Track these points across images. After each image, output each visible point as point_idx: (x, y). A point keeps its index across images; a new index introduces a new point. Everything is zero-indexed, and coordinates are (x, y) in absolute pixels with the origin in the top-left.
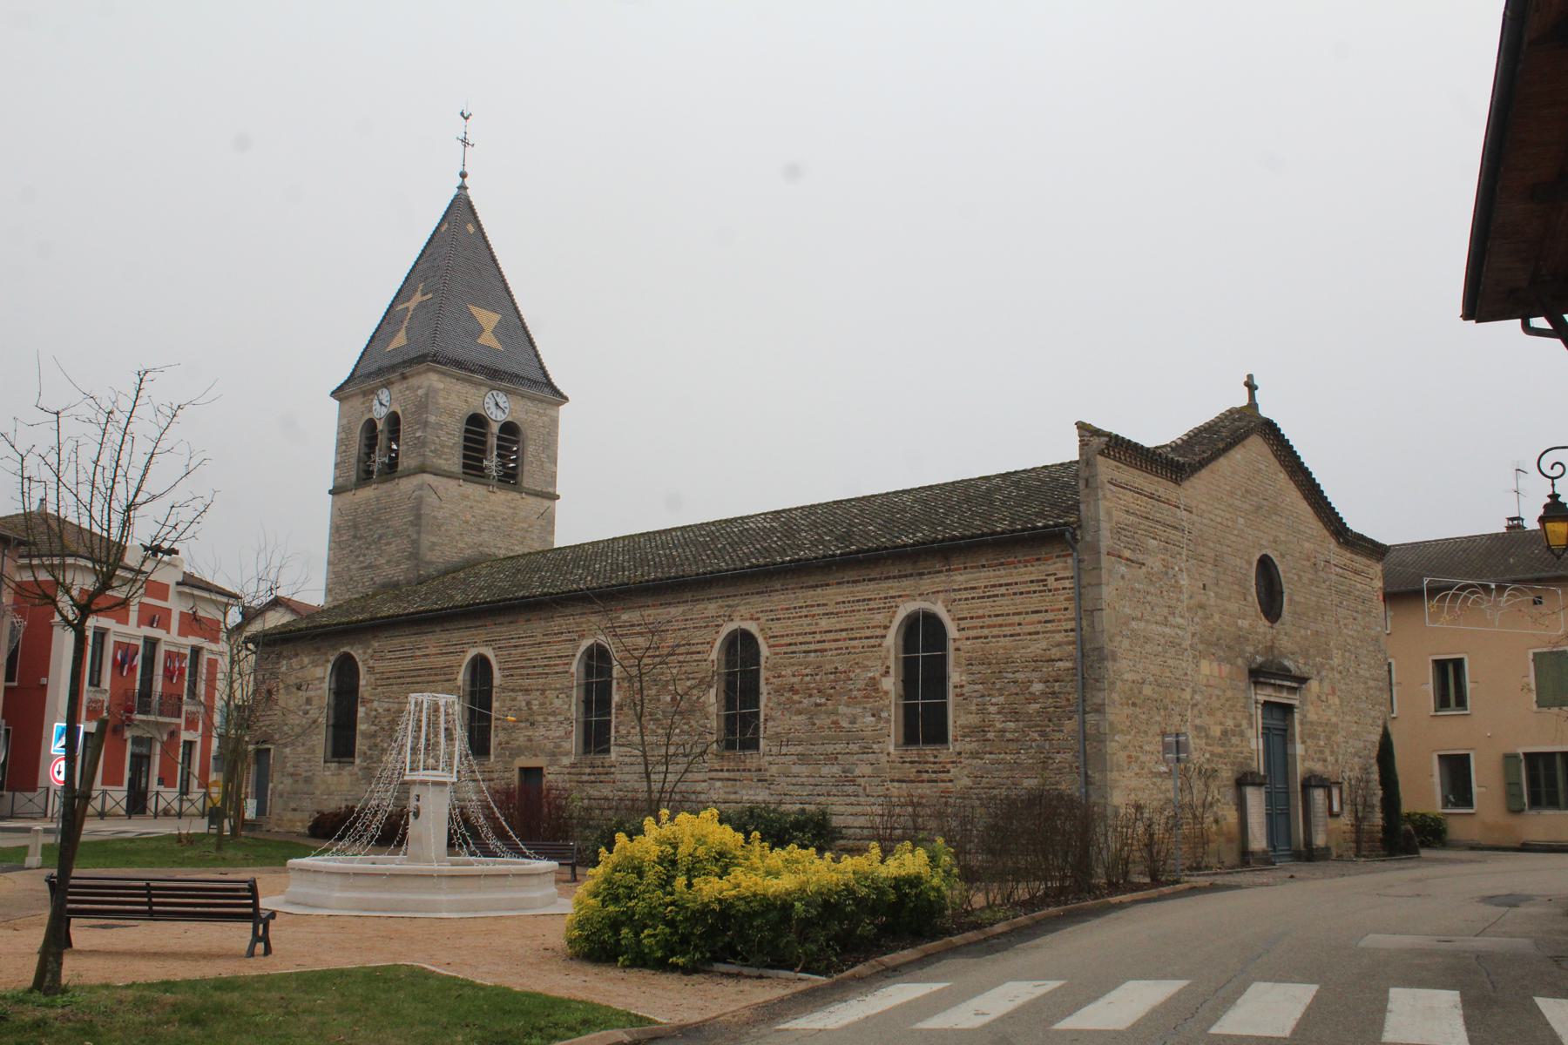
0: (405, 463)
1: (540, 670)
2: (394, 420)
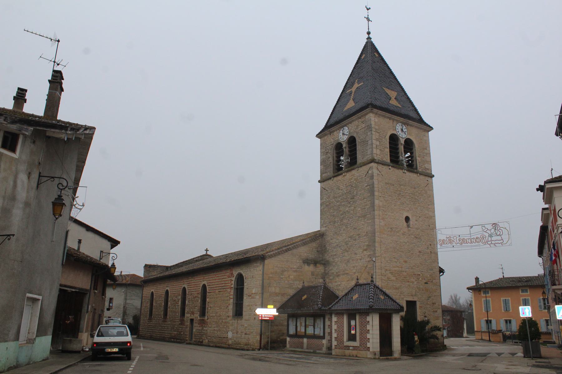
0: (360, 159)
2: (352, 141)
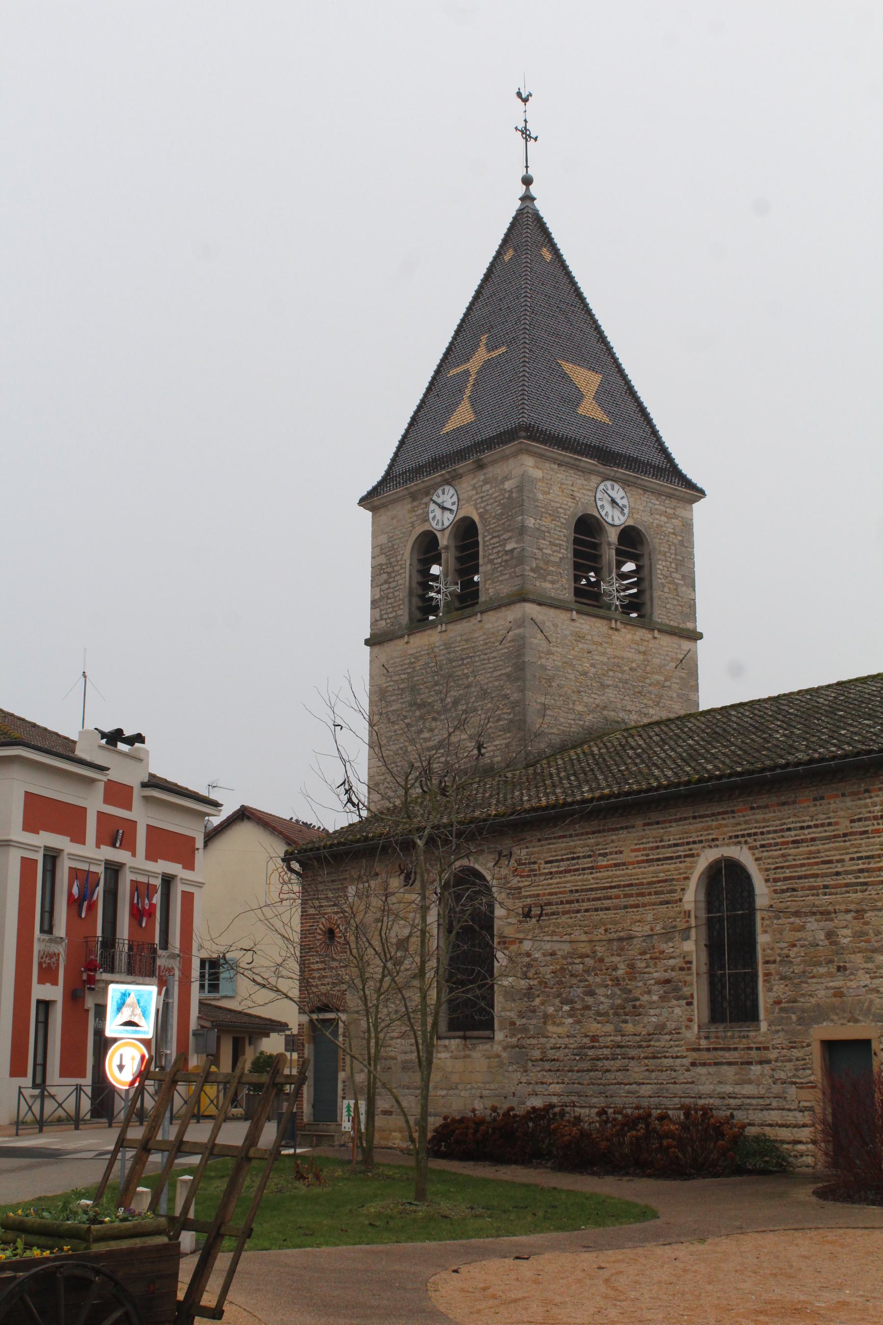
1: (850, 879)
2: (466, 531)
